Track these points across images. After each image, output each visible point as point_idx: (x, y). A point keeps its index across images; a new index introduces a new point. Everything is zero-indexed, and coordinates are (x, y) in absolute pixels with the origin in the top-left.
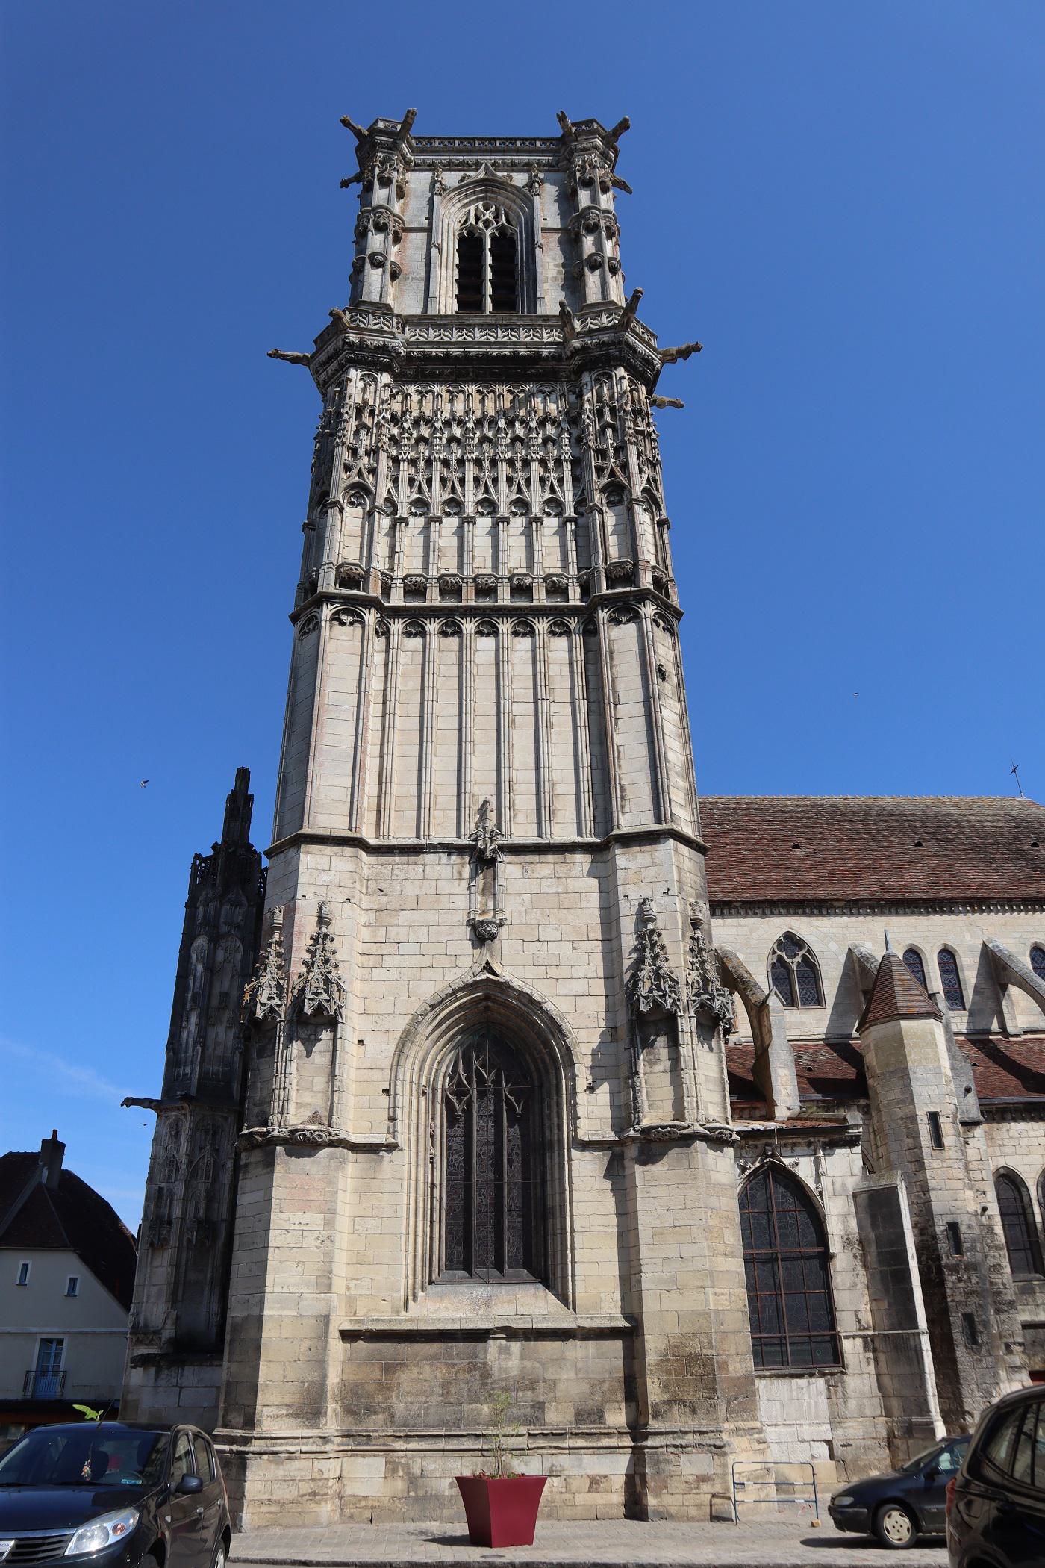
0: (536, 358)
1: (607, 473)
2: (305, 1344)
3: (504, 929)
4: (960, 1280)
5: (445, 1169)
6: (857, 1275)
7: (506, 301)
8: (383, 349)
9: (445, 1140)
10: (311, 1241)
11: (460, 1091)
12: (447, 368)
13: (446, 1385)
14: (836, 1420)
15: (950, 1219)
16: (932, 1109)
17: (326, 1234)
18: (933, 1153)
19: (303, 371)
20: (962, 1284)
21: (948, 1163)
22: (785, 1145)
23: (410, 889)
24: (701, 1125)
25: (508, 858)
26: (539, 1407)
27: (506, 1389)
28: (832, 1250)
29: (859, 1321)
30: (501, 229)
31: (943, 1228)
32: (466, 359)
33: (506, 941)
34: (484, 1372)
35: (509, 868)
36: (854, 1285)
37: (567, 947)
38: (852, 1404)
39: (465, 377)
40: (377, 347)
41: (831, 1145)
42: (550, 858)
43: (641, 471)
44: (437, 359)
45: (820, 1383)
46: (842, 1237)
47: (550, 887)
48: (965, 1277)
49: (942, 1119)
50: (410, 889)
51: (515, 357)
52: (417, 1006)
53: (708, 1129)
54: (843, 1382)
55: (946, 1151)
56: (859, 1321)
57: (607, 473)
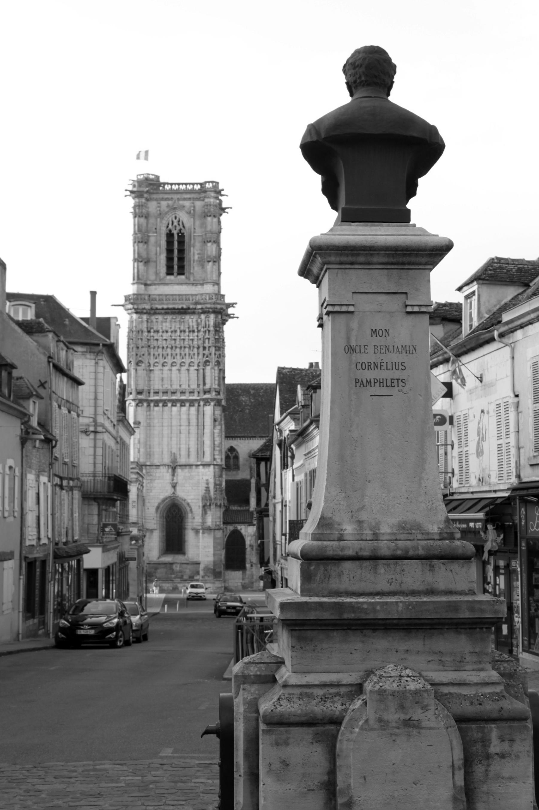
0: (189, 308)
1: (205, 356)
3: (177, 485)
7: (181, 271)
8: (144, 309)
11: (168, 517)
12: (163, 311)
14: (243, 579)
19: (122, 308)
23: (157, 475)
25: (178, 467)
26: (182, 576)
30: (180, 230)
32: (168, 309)
33: (178, 488)
34: (172, 570)
35: (179, 471)
37: (190, 488)
38: (247, 576)
41: (249, 525)
42: (188, 467)
43: (215, 354)
44: (160, 309)
45: (241, 572)
47: (187, 474)
50: (157, 475)
51: (182, 308)
52: (159, 501)
57: (205, 356)
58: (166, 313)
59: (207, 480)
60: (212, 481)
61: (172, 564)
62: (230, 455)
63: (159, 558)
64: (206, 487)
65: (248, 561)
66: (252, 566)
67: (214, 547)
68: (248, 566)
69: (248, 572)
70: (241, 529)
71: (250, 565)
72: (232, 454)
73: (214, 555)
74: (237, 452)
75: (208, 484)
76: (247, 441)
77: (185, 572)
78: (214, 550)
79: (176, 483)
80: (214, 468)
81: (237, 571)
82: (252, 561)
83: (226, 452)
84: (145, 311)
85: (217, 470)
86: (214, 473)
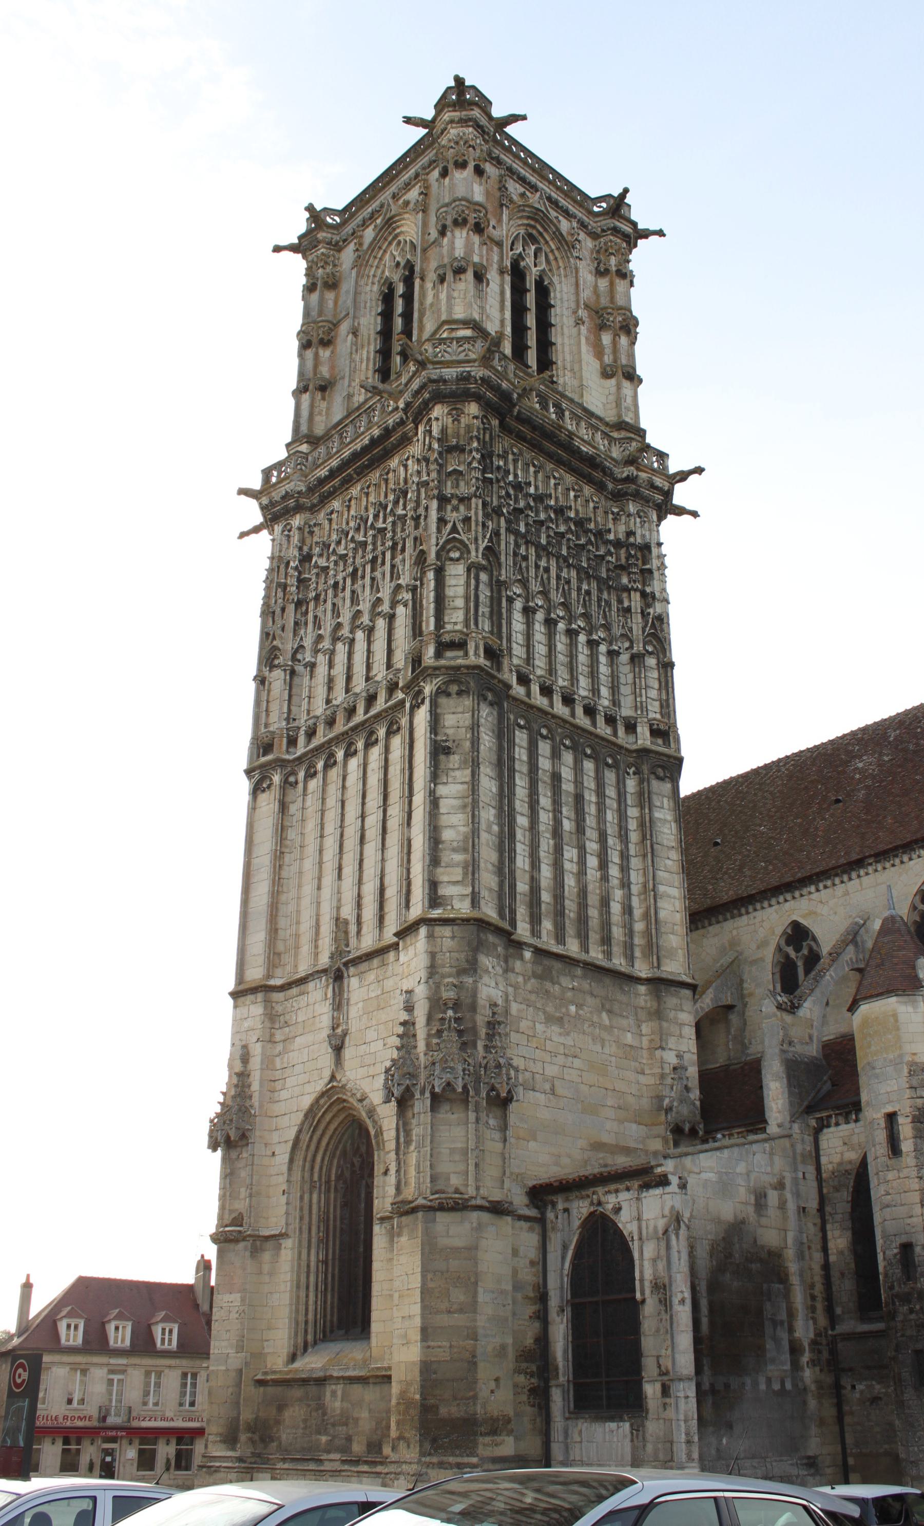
2: (230, 1390)
3: (347, 1038)
4: (911, 1311)
5: (337, 1247)
6: (661, 1320)
9: (338, 1223)
10: (234, 1315)
12: (336, 482)
13: (305, 1421)
15: (904, 1239)
16: (889, 1109)
17: (242, 1308)
18: (890, 1162)
20: (913, 1316)
21: (905, 1173)
22: (609, 1192)
24: (425, 1198)
26: (349, 1439)
27: (334, 1425)
28: (638, 1296)
29: (659, 1366)
31: (896, 1251)
36: (658, 1330)
38: (650, 1447)
39: (351, 481)
40: (283, 498)
41: (647, 1186)
46: (651, 1282)
48: (918, 1307)
49: (901, 1120)
53: (431, 1201)
54: (643, 1426)
55: (903, 1159)
56: (659, 1366)
58: (348, 482)
59: (409, 992)
60: (421, 992)
61: (322, 1381)
62: (793, 954)
63: (293, 1358)
64: (404, 1024)
65: (649, 1367)
66: (665, 1391)
67: (425, 1292)
68: (651, 1390)
69: (652, 1427)
70: (618, 1210)
71: (658, 1386)
72: (798, 949)
73: (426, 1332)
74: (814, 939)
75: (409, 1008)
76: (840, 889)
77: (357, 1420)
78: (426, 1308)
79: (345, 1034)
80: (430, 936)
81: (612, 1419)
82: (667, 1363)
83: (779, 949)
84: (291, 503)
85: (448, 943)
86: (433, 955)
